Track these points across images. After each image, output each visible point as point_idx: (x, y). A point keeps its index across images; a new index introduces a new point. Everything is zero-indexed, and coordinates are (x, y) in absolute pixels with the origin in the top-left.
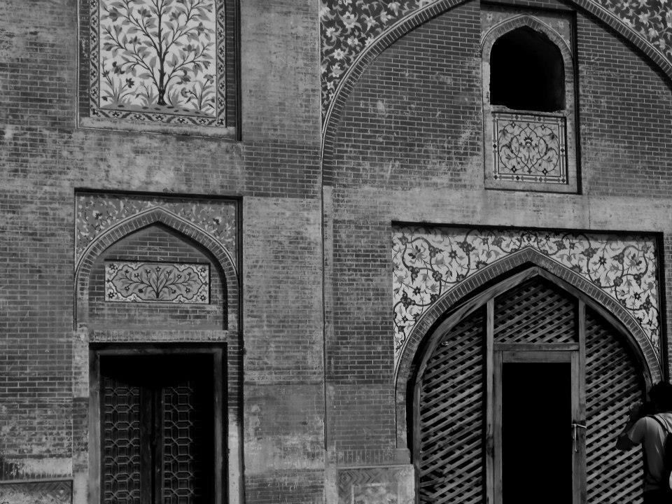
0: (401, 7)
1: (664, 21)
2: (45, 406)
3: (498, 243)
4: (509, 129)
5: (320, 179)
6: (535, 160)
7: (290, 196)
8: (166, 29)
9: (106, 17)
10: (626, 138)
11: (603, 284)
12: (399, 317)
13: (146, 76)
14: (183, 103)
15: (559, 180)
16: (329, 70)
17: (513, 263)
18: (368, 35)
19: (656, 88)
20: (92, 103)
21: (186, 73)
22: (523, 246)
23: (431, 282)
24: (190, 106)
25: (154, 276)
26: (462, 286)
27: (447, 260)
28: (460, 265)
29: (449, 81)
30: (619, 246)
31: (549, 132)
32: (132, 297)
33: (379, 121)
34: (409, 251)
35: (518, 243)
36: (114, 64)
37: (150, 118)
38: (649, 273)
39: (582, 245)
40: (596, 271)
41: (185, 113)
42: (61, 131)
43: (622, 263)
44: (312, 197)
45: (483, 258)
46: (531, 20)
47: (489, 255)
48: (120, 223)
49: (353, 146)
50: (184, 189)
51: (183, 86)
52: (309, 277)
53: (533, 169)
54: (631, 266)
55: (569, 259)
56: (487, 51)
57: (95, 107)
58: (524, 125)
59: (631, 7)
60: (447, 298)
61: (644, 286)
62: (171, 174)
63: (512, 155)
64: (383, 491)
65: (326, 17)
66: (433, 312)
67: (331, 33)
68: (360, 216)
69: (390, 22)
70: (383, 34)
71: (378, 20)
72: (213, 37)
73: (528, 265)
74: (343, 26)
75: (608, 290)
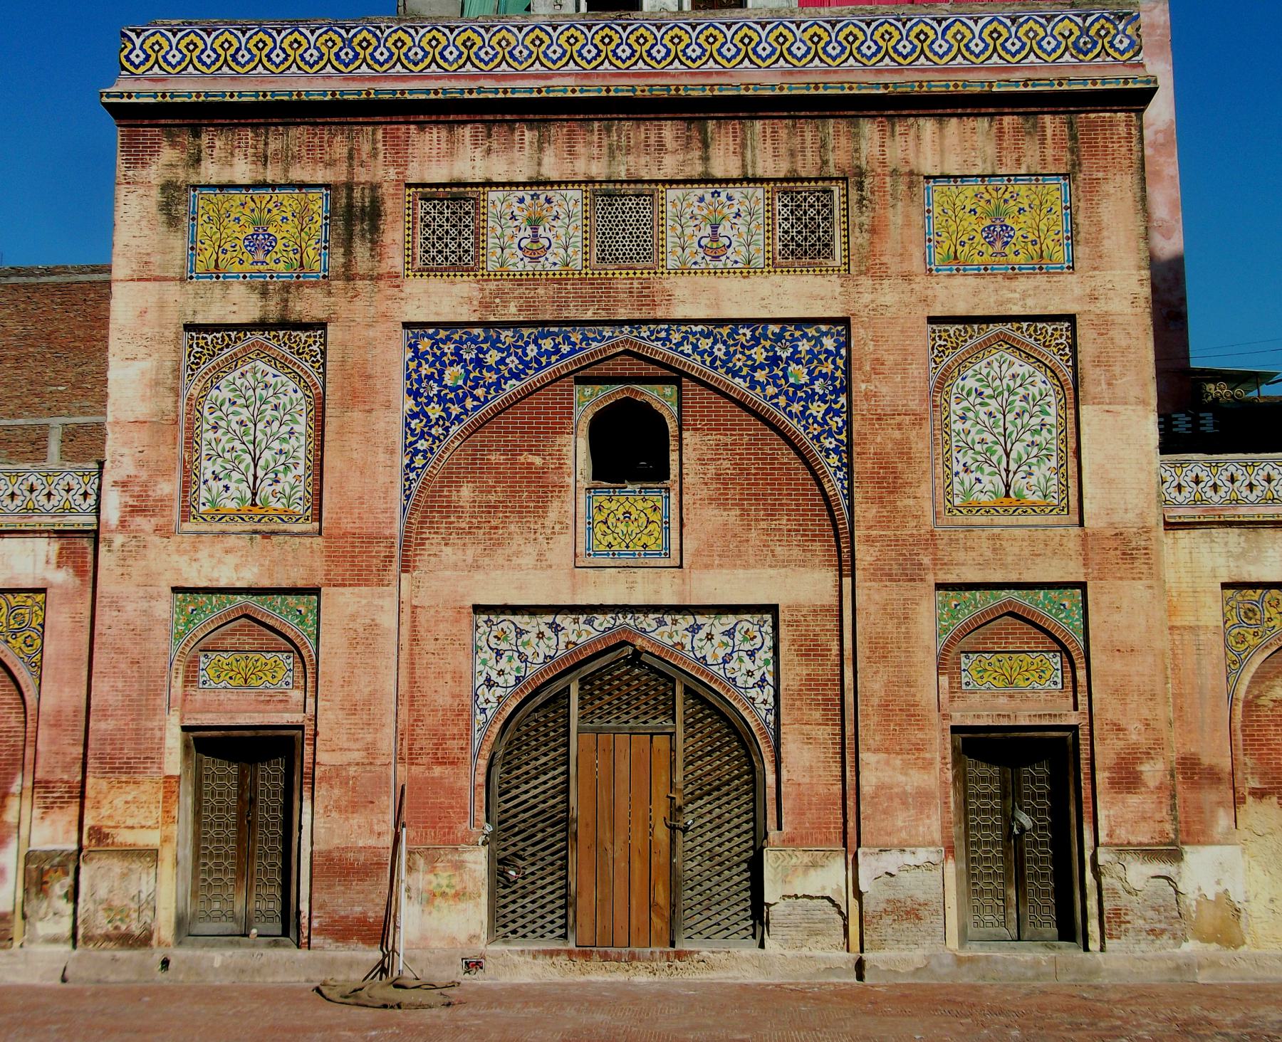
1: (786, 377)
3: (589, 622)
5: (395, 566)
8: (260, 436)
12: (481, 699)
14: (274, 504)
16: (412, 461)
18: (453, 423)
23: (516, 663)
24: (279, 506)
25: (243, 664)
29: (538, 461)
30: (730, 620)
38: (765, 648)
39: (686, 621)
40: (701, 648)
45: (573, 638)
47: (579, 635)
50: (266, 583)
55: (671, 636)
58: (622, 499)
59: (745, 365)
62: (255, 570)
63: (608, 531)
69: (475, 408)
70: (467, 420)
71: (463, 407)
72: (303, 439)
73: (623, 644)
74: (428, 417)
75: (715, 668)
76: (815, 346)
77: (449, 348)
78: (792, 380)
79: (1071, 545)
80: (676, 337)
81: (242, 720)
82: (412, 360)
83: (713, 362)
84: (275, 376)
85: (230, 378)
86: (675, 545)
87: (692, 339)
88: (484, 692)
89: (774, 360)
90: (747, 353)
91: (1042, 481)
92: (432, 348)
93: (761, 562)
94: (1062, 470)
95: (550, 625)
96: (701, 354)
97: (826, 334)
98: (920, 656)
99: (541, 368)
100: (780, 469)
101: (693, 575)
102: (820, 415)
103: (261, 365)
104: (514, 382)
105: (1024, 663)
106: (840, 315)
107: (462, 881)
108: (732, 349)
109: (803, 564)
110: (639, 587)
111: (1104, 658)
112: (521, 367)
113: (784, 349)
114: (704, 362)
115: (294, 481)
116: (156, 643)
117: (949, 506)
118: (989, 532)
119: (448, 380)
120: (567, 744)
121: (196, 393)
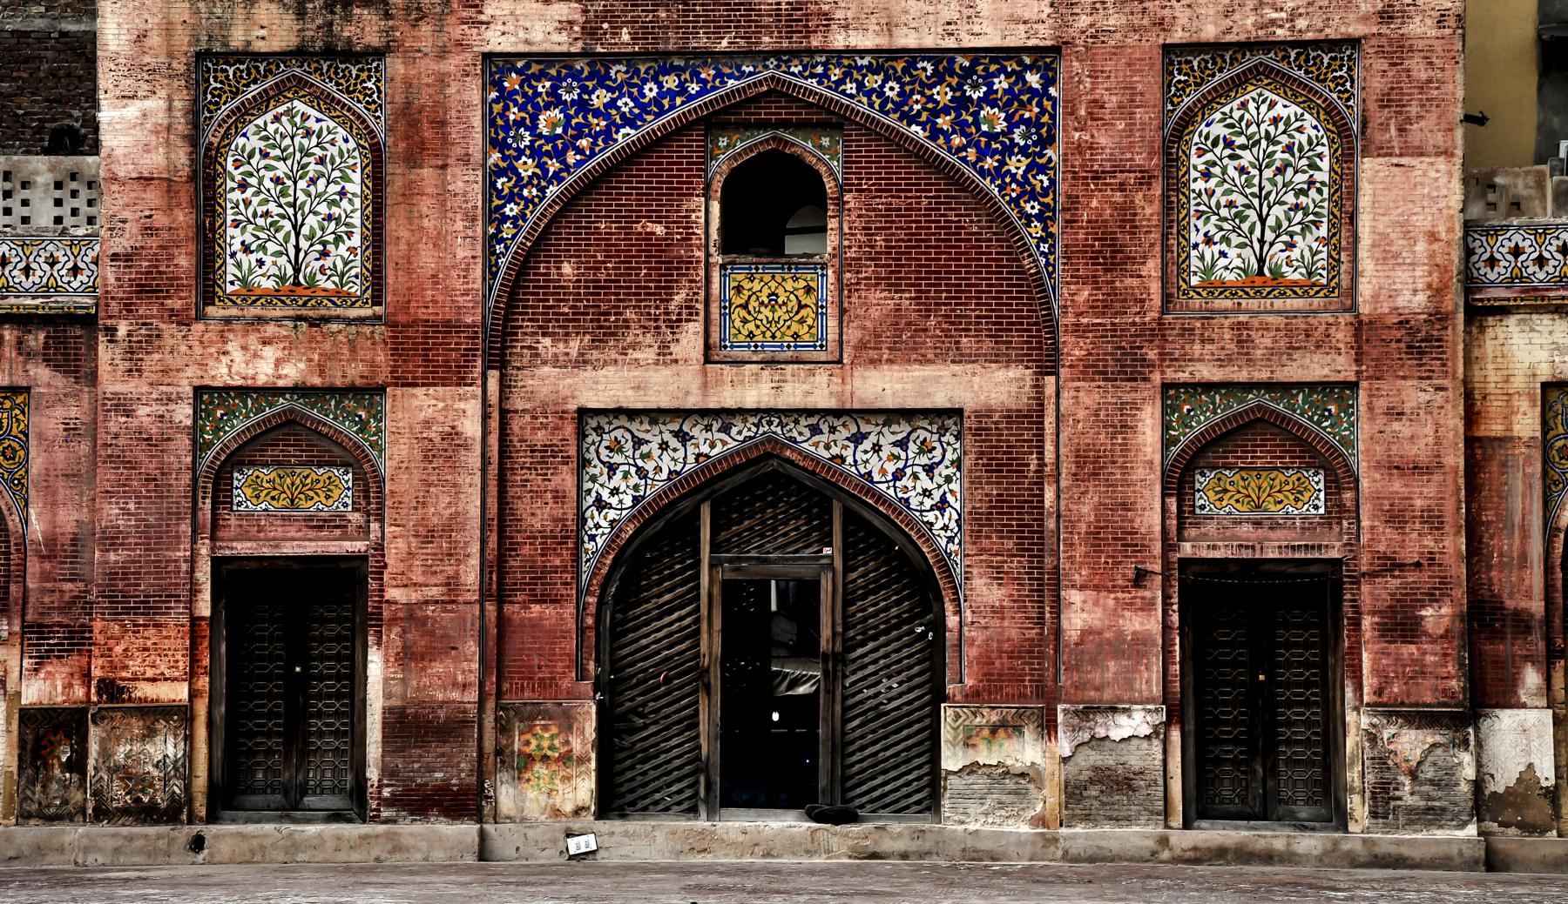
0: (594, 144)
1: (977, 124)
2: (161, 626)
3: (726, 429)
4: (746, 284)
6: (782, 322)
7: (443, 385)
8: (302, 197)
9: (233, 189)
10: (913, 285)
11: (876, 479)
12: (590, 523)
13: (278, 254)
14: (324, 283)
15: (815, 346)
16: (499, 231)
17: (745, 455)
18: (550, 183)
19: (961, 215)
20: (217, 289)
21: (325, 246)
22: (760, 432)
23: (634, 480)
24: (330, 285)
25: (288, 481)
26: (675, 485)
27: (656, 452)
28: (673, 459)
29: (659, 230)
30: (902, 429)
31: (802, 284)
32: (263, 506)
33: (564, 287)
34: (605, 444)
35: (754, 429)
36: (243, 243)
37: (283, 302)
38: (946, 462)
41: (324, 294)
42: (179, 324)
43: (906, 451)
44: (471, 385)
45: (705, 449)
46: (781, 140)
47: (713, 446)
48: (249, 423)
49: (529, 320)
51: (321, 262)
52: (463, 479)
53: (778, 334)
54: (919, 454)
55: (827, 447)
56: (717, 185)
57: (221, 293)
58: (767, 278)
60: (654, 500)
61: (938, 479)
62: (302, 366)
64: (554, 730)
65: (496, 165)
66: (634, 516)
67: (503, 184)
68: (537, 404)
69: (579, 164)
70: (570, 179)
71: (564, 162)
72: (357, 202)
73: (768, 456)
75: (883, 487)
76: (1016, 83)
77: (544, 86)
78: (984, 128)
79: (1340, 336)
80: (836, 74)
81: (288, 549)
82: (496, 101)
83: (883, 105)
84: (318, 120)
85: (260, 122)
86: (832, 336)
87: (856, 75)
88: (595, 517)
89: (961, 103)
90: (928, 93)
91: (1307, 254)
92: (521, 86)
93: (940, 356)
94: (1334, 241)
95: (676, 434)
96: (868, 94)
97: (1030, 68)
98: (1140, 473)
99: (662, 112)
100: (969, 240)
101: (856, 374)
102: (1020, 172)
103: (299, 106)
104: (627, 130)
105: (1277, 482)
106: (1049, 43)
107: (567, 742)
108: (908, 88)
109: (995, 358)
110: (788, 387)
111: (1378, 476)
112: (636, 111)
113: (975, 87)
114: (871, 105)
115: (348, 252)
116: (178, 456)
117: (1184, 287)
118: (1233, 319)
119: (543, 129)
120: (697, 576)
121: (215, 141)
